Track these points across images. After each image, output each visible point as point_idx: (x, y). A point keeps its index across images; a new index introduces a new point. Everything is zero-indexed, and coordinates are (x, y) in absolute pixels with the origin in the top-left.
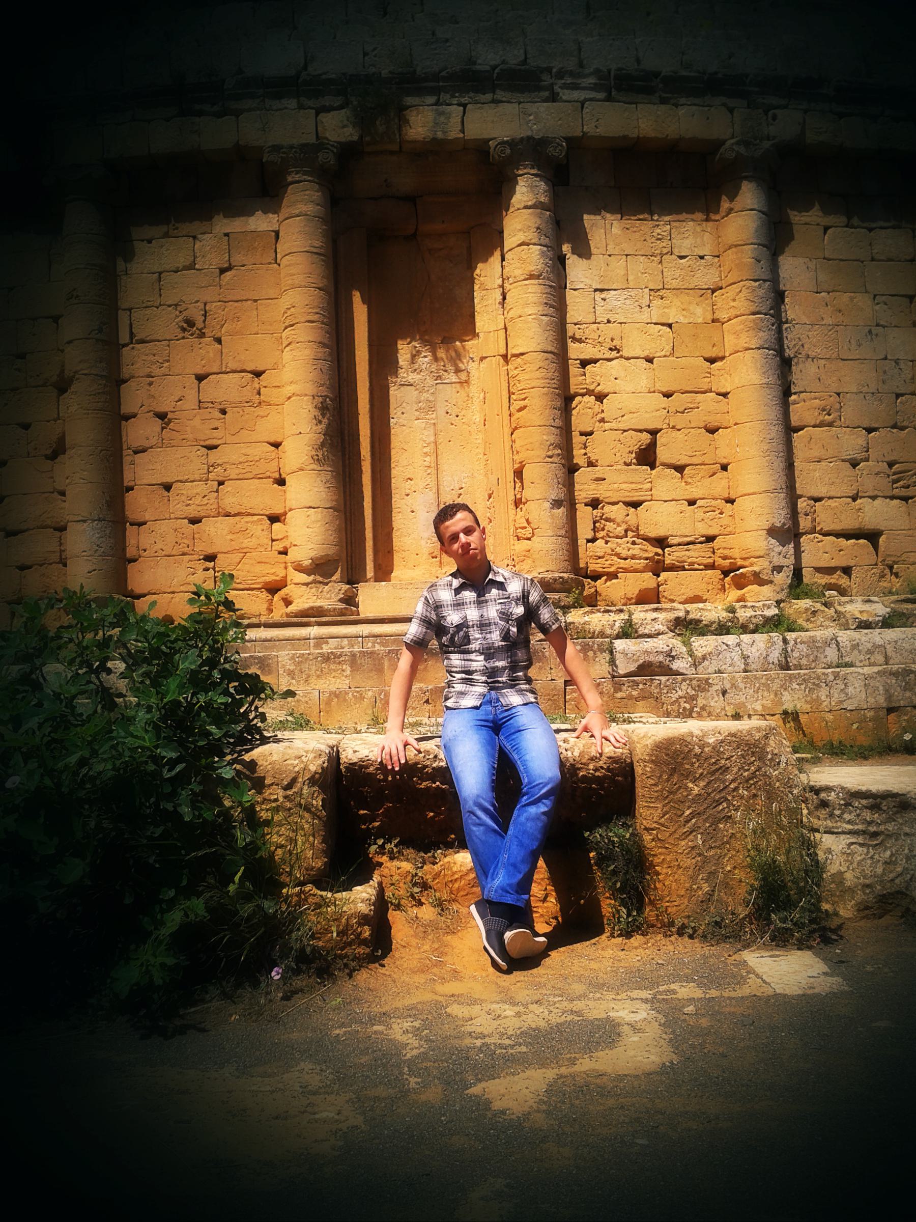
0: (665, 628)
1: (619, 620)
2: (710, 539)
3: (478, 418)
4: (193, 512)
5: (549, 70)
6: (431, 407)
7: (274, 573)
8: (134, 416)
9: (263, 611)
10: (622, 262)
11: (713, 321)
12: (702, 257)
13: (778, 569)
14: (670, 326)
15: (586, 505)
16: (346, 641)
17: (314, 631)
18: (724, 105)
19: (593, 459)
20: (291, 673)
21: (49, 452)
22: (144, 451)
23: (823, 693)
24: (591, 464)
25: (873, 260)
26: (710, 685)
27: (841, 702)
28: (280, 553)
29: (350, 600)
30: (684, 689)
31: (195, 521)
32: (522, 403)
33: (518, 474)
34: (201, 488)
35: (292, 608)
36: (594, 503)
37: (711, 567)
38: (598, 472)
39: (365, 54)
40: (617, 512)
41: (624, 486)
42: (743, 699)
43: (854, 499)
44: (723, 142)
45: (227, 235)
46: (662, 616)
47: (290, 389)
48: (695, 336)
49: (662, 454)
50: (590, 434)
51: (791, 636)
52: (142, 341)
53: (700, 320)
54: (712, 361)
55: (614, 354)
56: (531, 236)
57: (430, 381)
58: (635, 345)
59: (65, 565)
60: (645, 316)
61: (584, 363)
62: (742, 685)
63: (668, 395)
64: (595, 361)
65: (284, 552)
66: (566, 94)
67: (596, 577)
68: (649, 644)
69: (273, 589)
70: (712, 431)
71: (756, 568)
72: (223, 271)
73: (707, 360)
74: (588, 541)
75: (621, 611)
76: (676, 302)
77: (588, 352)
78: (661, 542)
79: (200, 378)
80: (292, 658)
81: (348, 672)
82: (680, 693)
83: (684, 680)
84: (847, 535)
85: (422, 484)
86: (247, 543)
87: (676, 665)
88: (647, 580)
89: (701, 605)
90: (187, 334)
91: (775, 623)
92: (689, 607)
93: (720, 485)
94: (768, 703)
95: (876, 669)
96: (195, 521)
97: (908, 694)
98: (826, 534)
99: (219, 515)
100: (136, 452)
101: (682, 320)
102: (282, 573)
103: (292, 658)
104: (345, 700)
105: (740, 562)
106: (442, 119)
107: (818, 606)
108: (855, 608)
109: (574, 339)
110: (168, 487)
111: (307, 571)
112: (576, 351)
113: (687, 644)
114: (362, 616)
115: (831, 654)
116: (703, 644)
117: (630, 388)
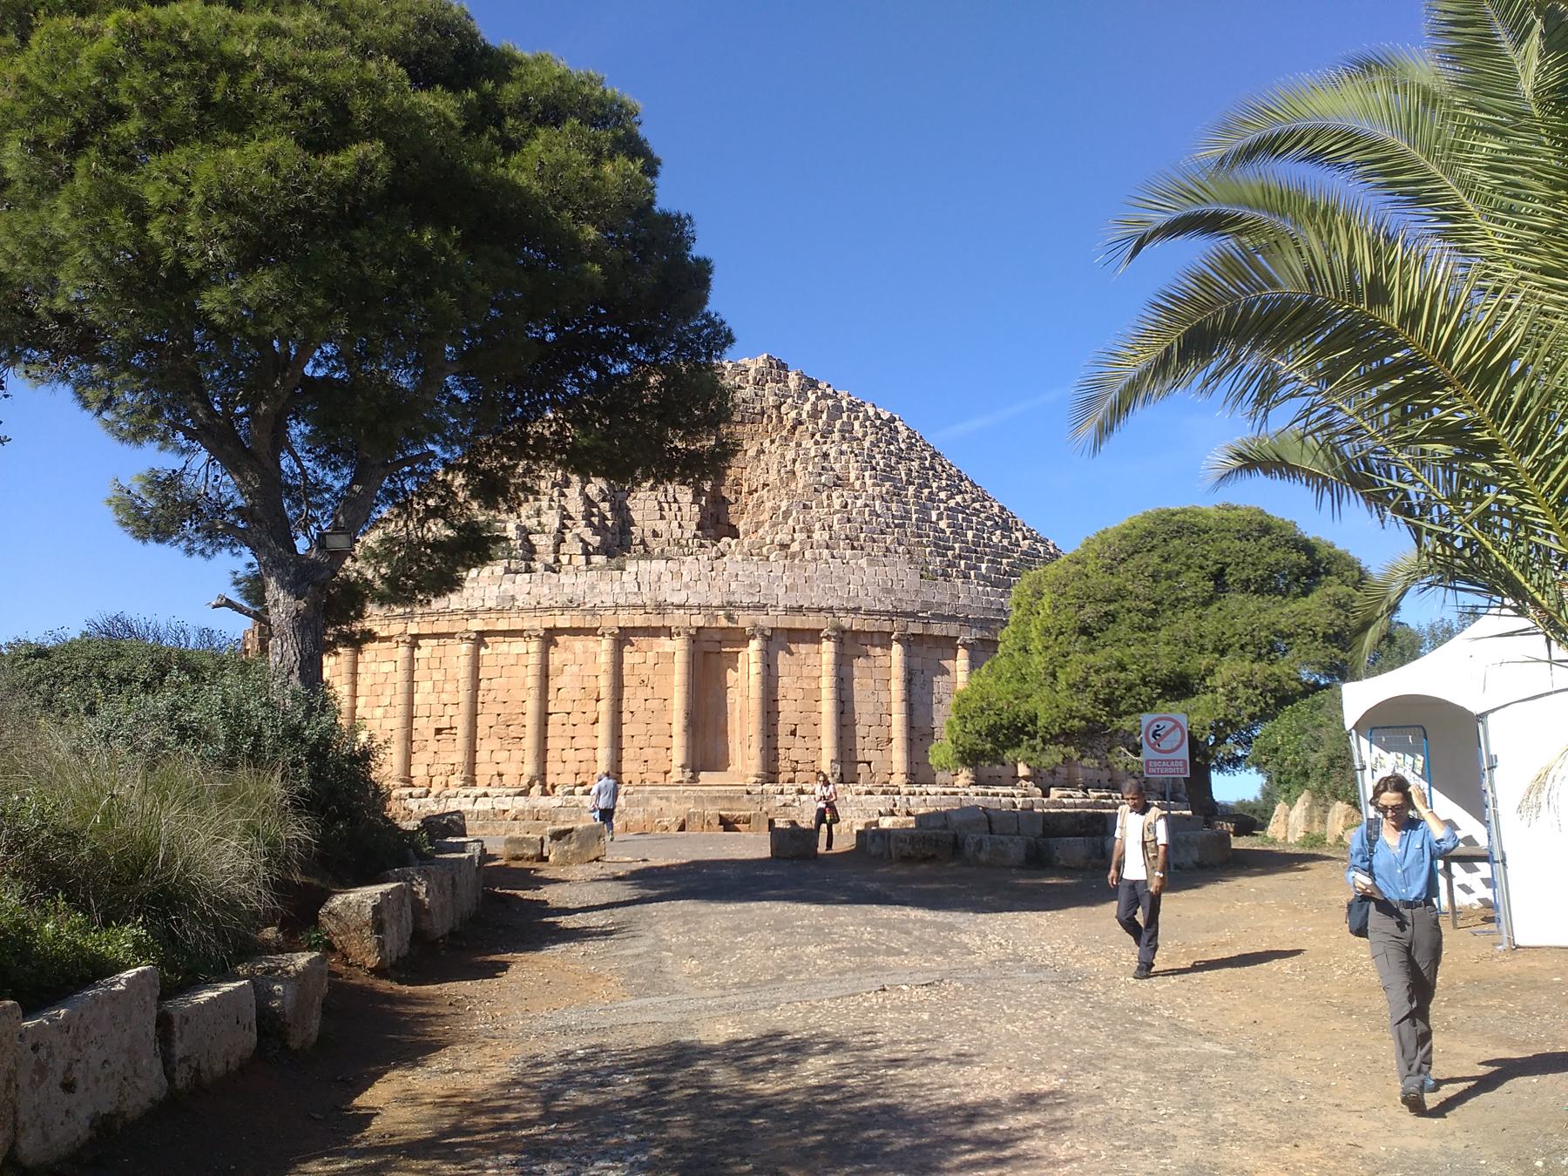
17: (681, 788)
69: (666, 773)
88: (792, 775)
93: (816, 743)
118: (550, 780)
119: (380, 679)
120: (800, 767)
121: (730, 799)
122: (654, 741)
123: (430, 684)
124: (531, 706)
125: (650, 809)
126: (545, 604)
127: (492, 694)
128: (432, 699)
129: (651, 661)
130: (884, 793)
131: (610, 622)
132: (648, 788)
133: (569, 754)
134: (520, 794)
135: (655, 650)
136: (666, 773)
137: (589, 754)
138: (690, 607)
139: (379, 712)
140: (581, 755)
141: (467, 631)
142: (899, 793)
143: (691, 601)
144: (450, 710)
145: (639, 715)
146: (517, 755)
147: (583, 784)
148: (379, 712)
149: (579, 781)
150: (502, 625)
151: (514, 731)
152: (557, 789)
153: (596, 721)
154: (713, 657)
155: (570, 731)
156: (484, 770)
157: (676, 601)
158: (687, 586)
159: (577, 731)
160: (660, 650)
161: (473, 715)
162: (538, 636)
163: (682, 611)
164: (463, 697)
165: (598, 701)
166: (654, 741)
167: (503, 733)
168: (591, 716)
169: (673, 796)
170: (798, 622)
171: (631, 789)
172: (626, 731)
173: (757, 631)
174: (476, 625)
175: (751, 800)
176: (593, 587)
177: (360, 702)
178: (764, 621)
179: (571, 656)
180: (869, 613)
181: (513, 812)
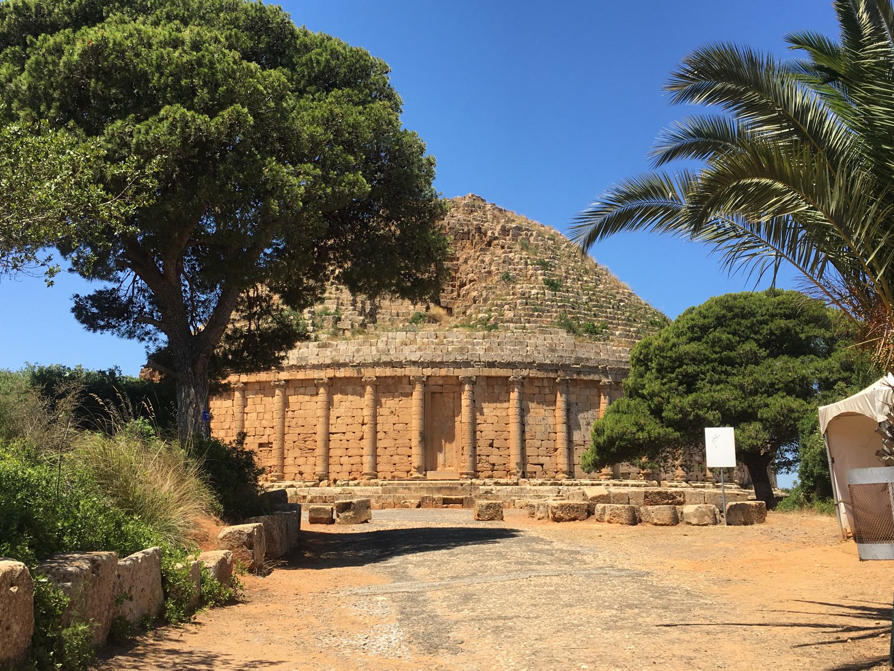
1: (482, 482)
4: (391, 454)
7: (408, 468)
13: (518, 472)
17: (418, 482)
29: (425, 475)
33: (463, 448)
34: (393, 449)
36: (479, 455)
47: (413, 429)
56: (467, 397)
69: (408, 472)
78: (494, 465)
84: (536, 464)
93: (507, 452)
108: (533, 481)
116: (499, 488)
118: (332, 476)
120: (495, 468)
122: (400, 451)
123: (255, 414)
124: (320, 429)
126: (328, 361)
127: (295, 421)
128: (256, 424)
131: (369, 374)
132: (396, 482)
133: (345, 460)
134: (313, 486)
136: (408, 472)
137: (358, 459)
140: (352, 460)
141: (279, 381)
142: (561, 485)
144: (268, 431)
146: (311, 460)
147: (355, 479)
149: (351, 477)
151: (310, 444)
152: (338, 482)
153: (362, 438)
154: (437, 395)
156: (290, 470)
157: (413, 359)
158: (420, 349)
159: (351, 444)
162: (323, 385)
164: (277, 422)
165: (363, 425)
167: (302, 446)
168: (359, 435)
169: (413, 487)
171: (385, 482)
172: (380, 444)
173: (469, 380)
175: (464, 489)
176: (358, 351)
178: (470, 372)
181: (309, 497)
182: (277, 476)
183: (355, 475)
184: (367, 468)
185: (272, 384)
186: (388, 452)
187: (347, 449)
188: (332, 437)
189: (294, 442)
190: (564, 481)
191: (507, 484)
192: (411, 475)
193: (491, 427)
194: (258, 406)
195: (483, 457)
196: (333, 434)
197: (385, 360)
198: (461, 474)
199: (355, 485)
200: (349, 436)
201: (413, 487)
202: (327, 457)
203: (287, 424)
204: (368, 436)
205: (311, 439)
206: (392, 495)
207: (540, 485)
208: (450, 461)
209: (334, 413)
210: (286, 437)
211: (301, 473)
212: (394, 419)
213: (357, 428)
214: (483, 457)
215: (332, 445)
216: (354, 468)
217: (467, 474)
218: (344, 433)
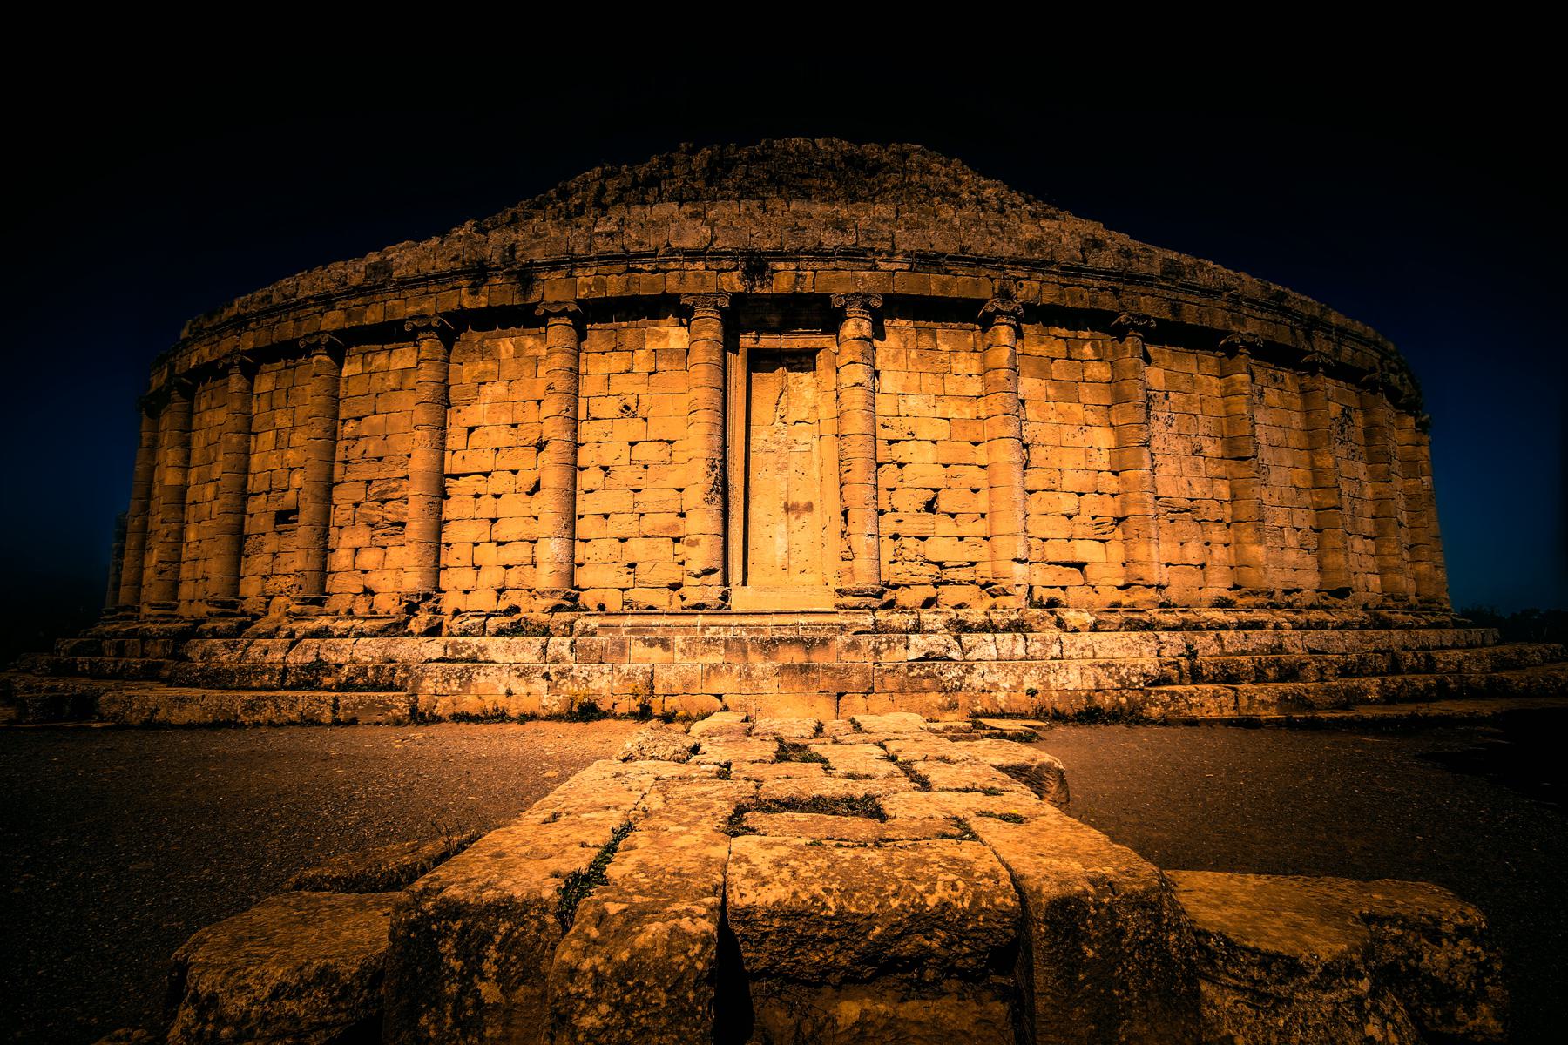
0: (941, 626)
1: (911, 619)
2: (973, 564)
3: (817, 476)
5: (872, 250)
6: (785, 467)
7: (676, 577)
8: (587, 468)
9: (667, 604)
10: (917, 376)
11: (977, 418)
12: (970, 376)
14: (948, 419)
15: (890, 537)
16: (722, 629)
17: (700, 620)
18: (988, 276)
19: (895, 507)
20: (683, 651)
21: (529, 490)
22: (592, 491)
23: (1051, 678)
24: (894, 510)
25: (1084, 381)
26: (974, 669)
27: (1064, 684)
28: (679, 564)
29: (725, 597)
30: (956, 672)
31: (623, 540)
32: (848, 468)
33: (845, 514)
34: (628, 518)
35: (686, 603)
36: (895, 537)
37: (973, 582)
38: (899, 516)
39: (751, 236)
40: (911, 544)
41: (916, 526)
42: (996, 679)
43: (1069, 540)
44: (983, 302)
45: (654, 350)
46: (939, 617)
48: (965, 428)
49: (943, 504)
50: (894, 489)
51: (1030, 636)
52: (595, 419)
53: (968, 417)
54: (976, 444)
55: (910, 437)
57: (785, 450)
58: (925, 432)
59: (535, 566)
60: (932, 413)
61: (891, 442)
62: (996, 670)
63: (946, 466)
64: (898, 441)
65: (682, 563)
66: (883, 266)
67: (896, 587)
68: (933, 638)
69: (675, 587)
70: (975, 491)
71: (1004, 586)
72: (650, 374)
73: (972, 443)
74: (891, 562)
75: (913, 613)
76: (953, 404)
77: (893, 435)
78: (940, 565)
79: (632, 444)
80: (684, 640)
81: (723, 652)
82: (954, 674)
83: (957, 665)
84: (1065, 565)
85: (778, 520)
86: (657, 556)
87: (952, 654)
89: (967, 610)
90: (624, 415)
91: (1017, 627)
92: (961, 612)
93: (981, 528)
94: (1014, 684)
95: (1089, 662)
96: (623, 540)
97: (1110, 681)
98: (1049, 563)
99: (639, 536)
100: (586, 492)
101: (957, 416)
102: (680, 577)
103: (684, 640)
104: (720, 671)
105: (992, 581)
106: (800, 279)
107: (1046, 614)
109: (884, 426)
110: (606, 516)
111: (697, 576)
112: (883, 434)
113: (958, 639)
114: (733, 610)
115: (1056, 649)
116: (966, 638)
117: (921, 460)
118: (450, 602)
119: (213, 437)
121: (808, 645)
124: (421, 462)
125: (625, 668)
127: (362, 444)
129: (642, 367)
130: (1131, 626)
132: (629, 620)
133: (487, 553)
135: (649, 346)
137: (518, 553)
138: (719, 255)
139: (210, 491)
141: (319, 332)
143: (718, 245)
145: (625, 475)
146: (396, 555)
148: (210, 491)
149: (503, 605)
150: (373, 316)
151: (392, 511)
153: (536, 488)
155: (487, 507)
156: (344, 585)
157: (689, 243)
160: (661, 345)
161: (328, 486)
163: (700, 266)
166: (647, 524)
167: (376, 514)
168: (527, 479)
170: (934, 285)
171: (594, 623)
174: (333, 320)
175: (853, 646)
177: (193, 475)
178: (865, 280)
179: (491, 366)
180: (1066, 271)
182: (304, 601)
183: (513, 598)
184: (546, 578)
185: (301, 345)
186: (616, 527)
187: (494, 521)
188: (454, 487)
189: (357, 505)
190: (1155, 614)
191: (989, 627)
192: (683, 598)
193: (930, 454)
194: (279, 413)
195: (905, 542)
196: (456, 477)
197: (606, 249)
198: (841, 592)
199: (501, 632)
200: (500, 482)
201: (678, 639)
202: (436, 543)
203: (340, 455)
204: (553, 479)
205: (397, 495)
206: (606, 668)
207: (1095, 629)
208: (803, 556)
209: (458, 421)
210: (337, 494)
211: (368, 592)
212: (634, 429)
213: (524, 460)
214: (905, 542)
215: (451, 509)
216: (513, 578)
217: (859, 593)
218: (486, 474)
